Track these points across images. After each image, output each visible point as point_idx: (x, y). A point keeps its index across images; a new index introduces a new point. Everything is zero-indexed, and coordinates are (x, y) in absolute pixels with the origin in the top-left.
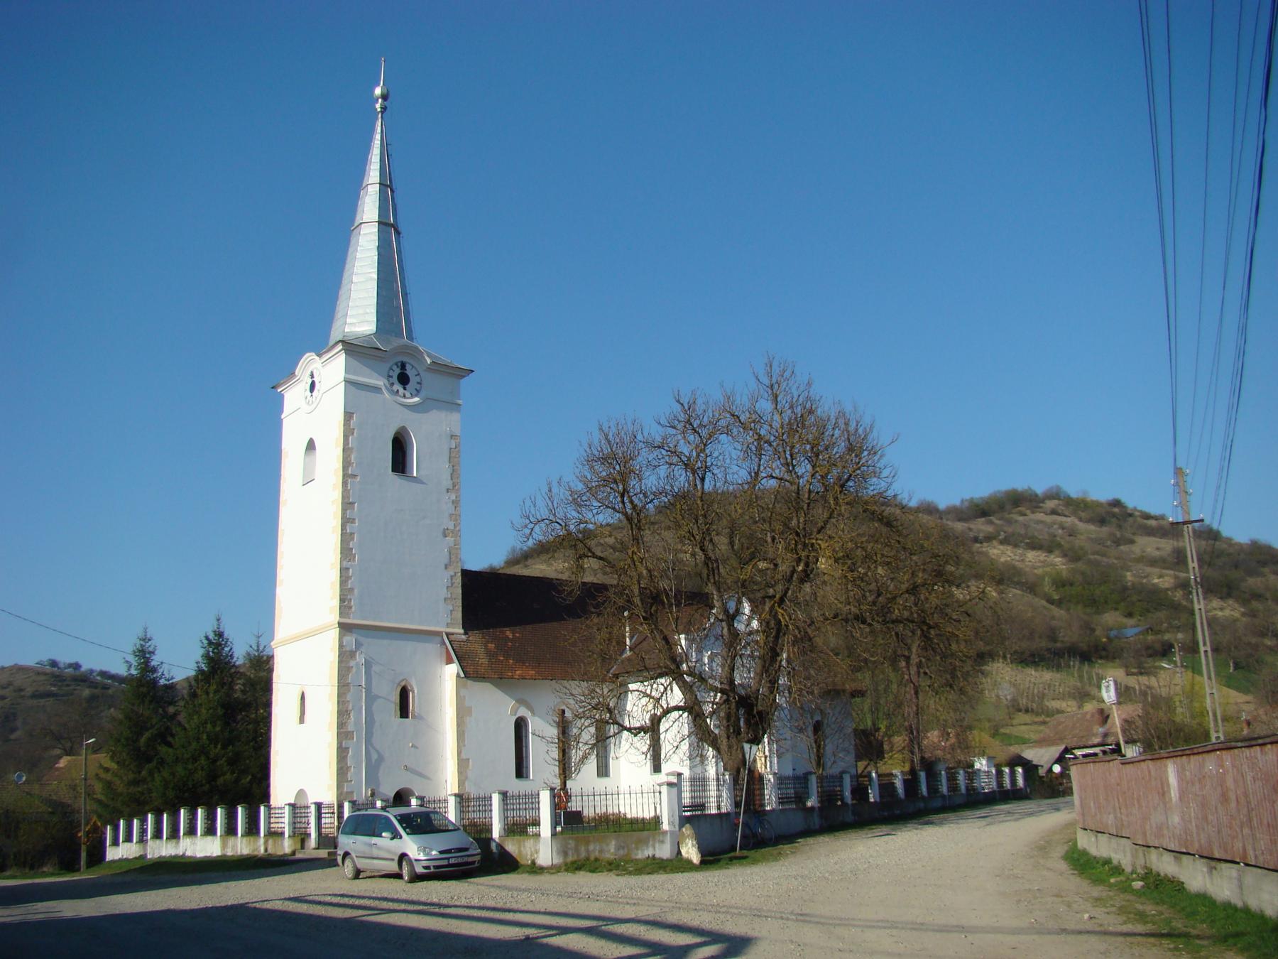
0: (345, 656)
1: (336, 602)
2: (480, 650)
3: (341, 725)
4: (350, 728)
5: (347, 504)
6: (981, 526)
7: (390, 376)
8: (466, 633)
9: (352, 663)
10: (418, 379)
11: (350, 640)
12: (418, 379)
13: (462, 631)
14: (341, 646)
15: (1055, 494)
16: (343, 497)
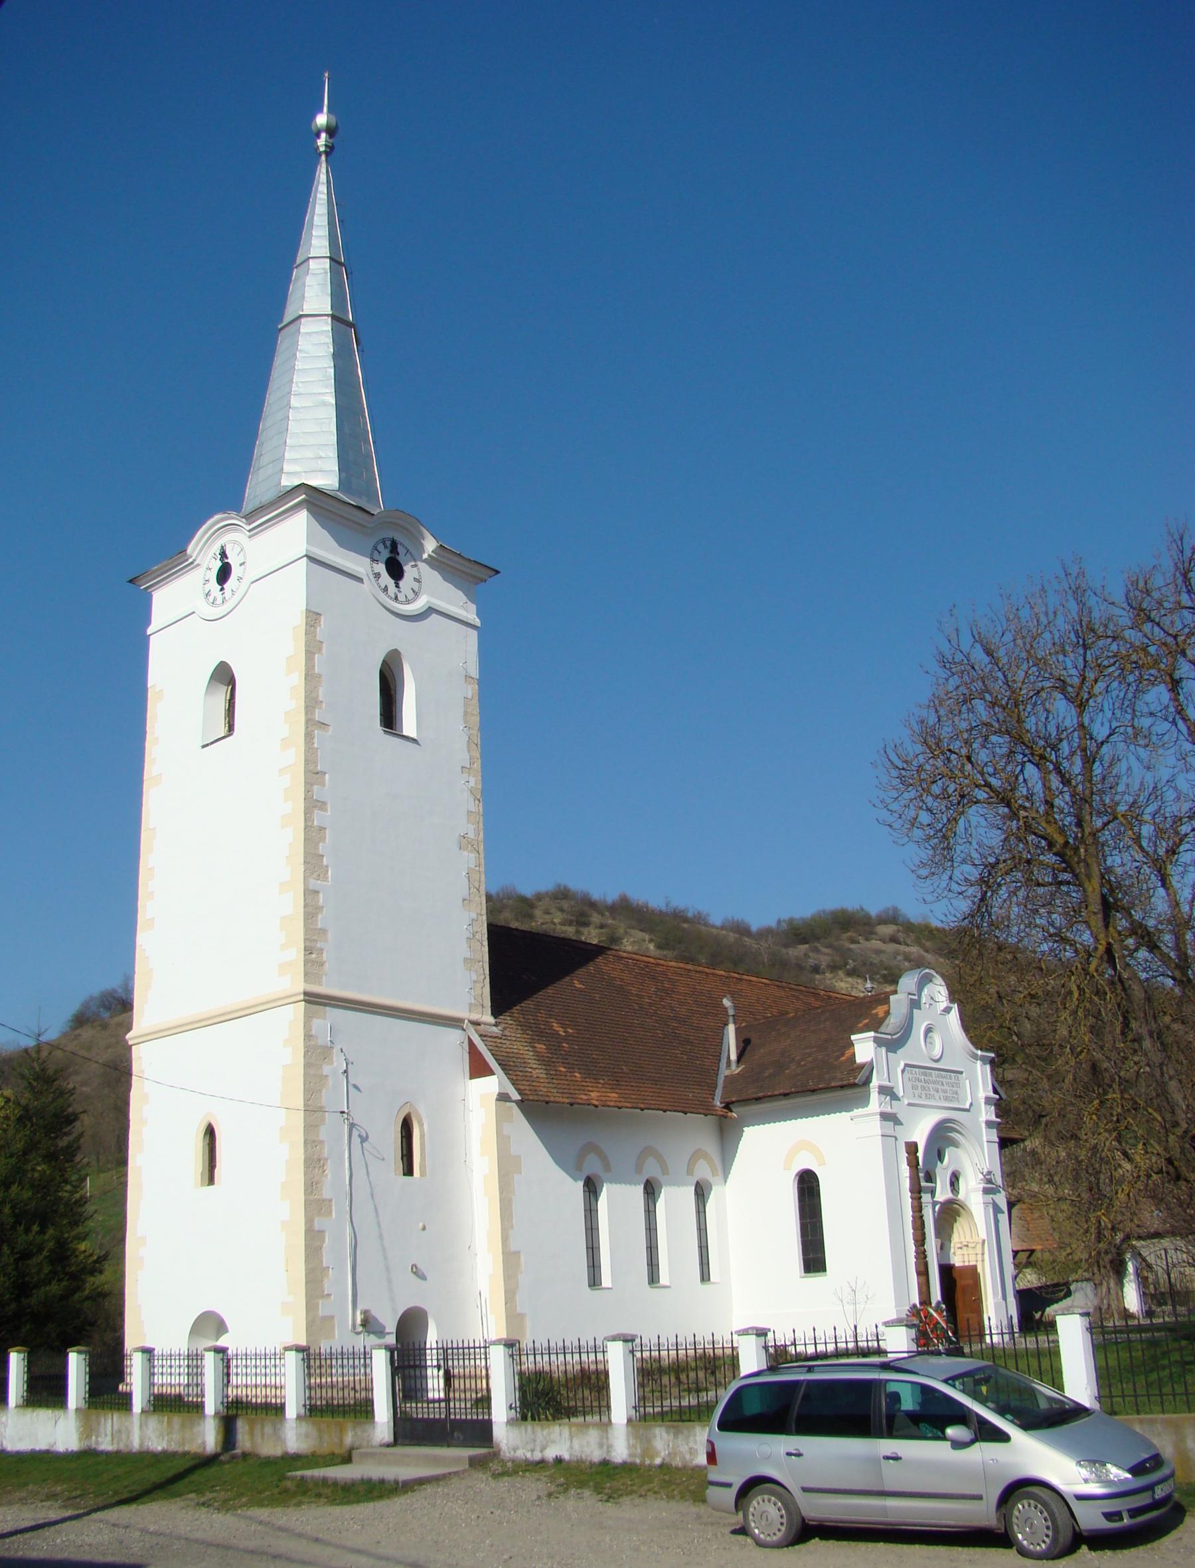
0: (316, 1054)
1: (296, 954)
3: (311, 1186)
4: (327, 1193)
5: (313, 776)
6: (798, 951)
9: (326, 1069)
14: (308, 1036)
15: (891, 918)
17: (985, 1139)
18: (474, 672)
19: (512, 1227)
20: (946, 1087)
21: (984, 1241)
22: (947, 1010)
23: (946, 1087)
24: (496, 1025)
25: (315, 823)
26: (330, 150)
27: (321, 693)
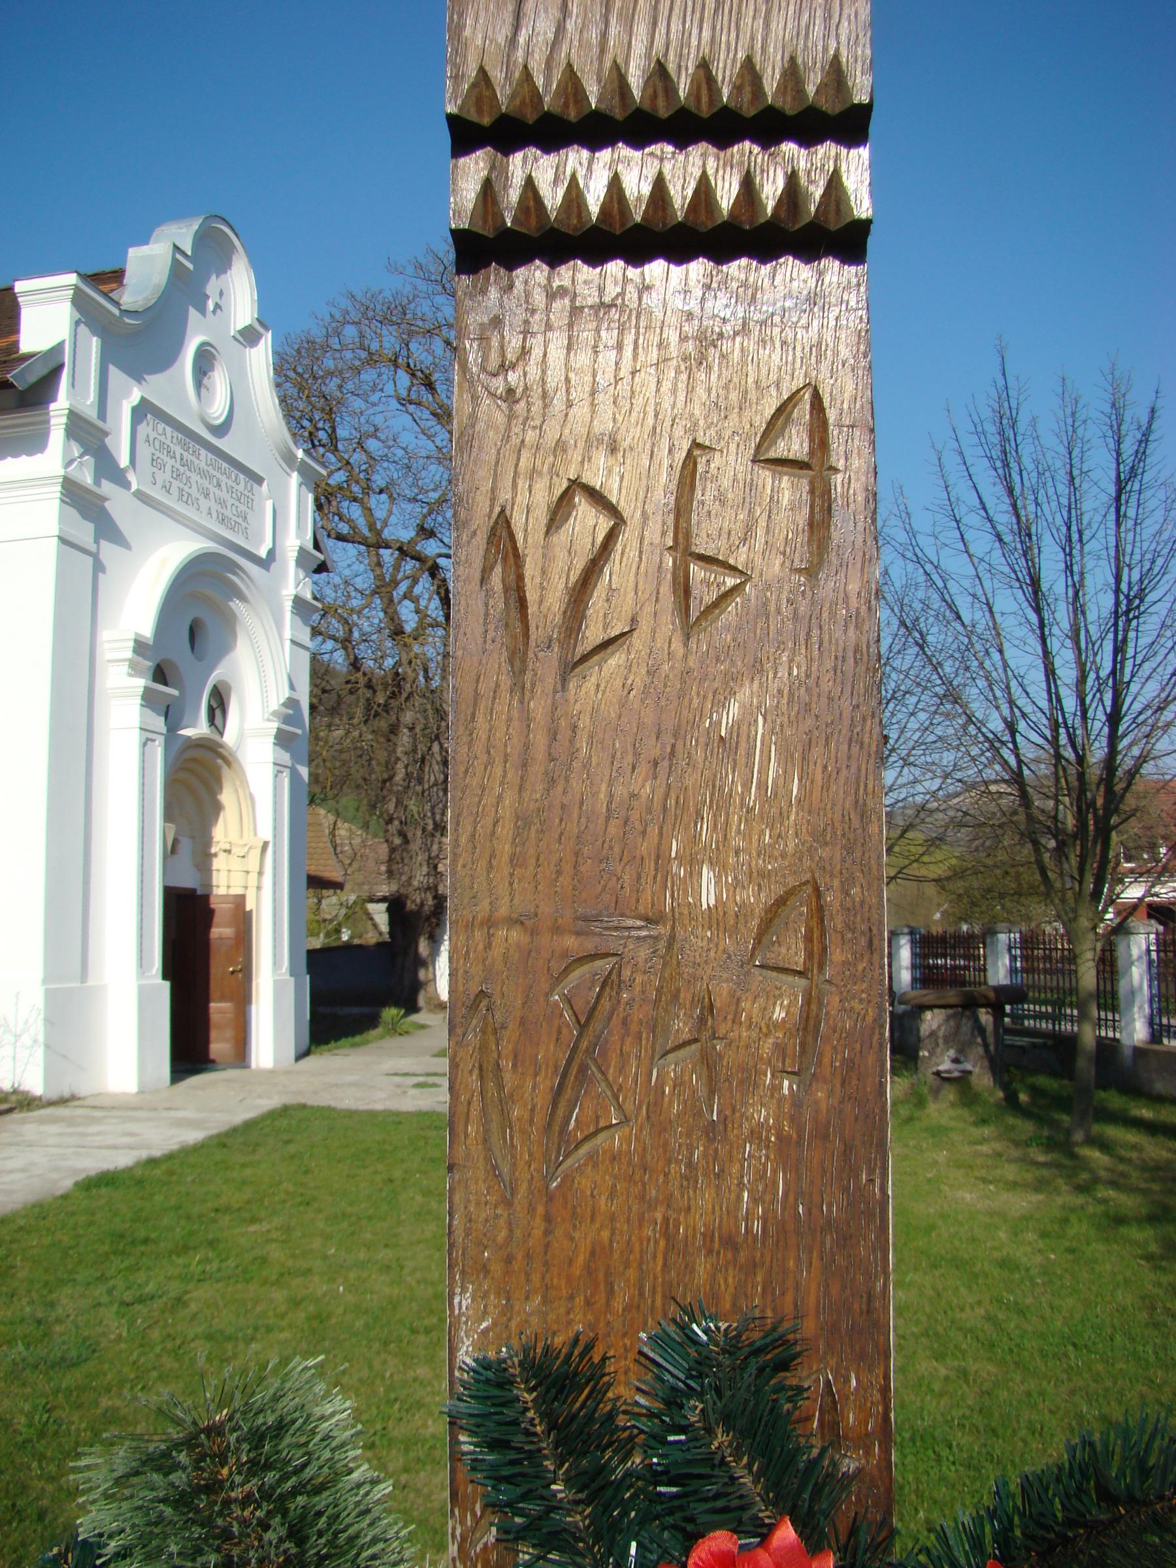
17: (288, 634)
20: (224, 495)
21: (266, 844)
22: (249, 336)
23: (224, 495)
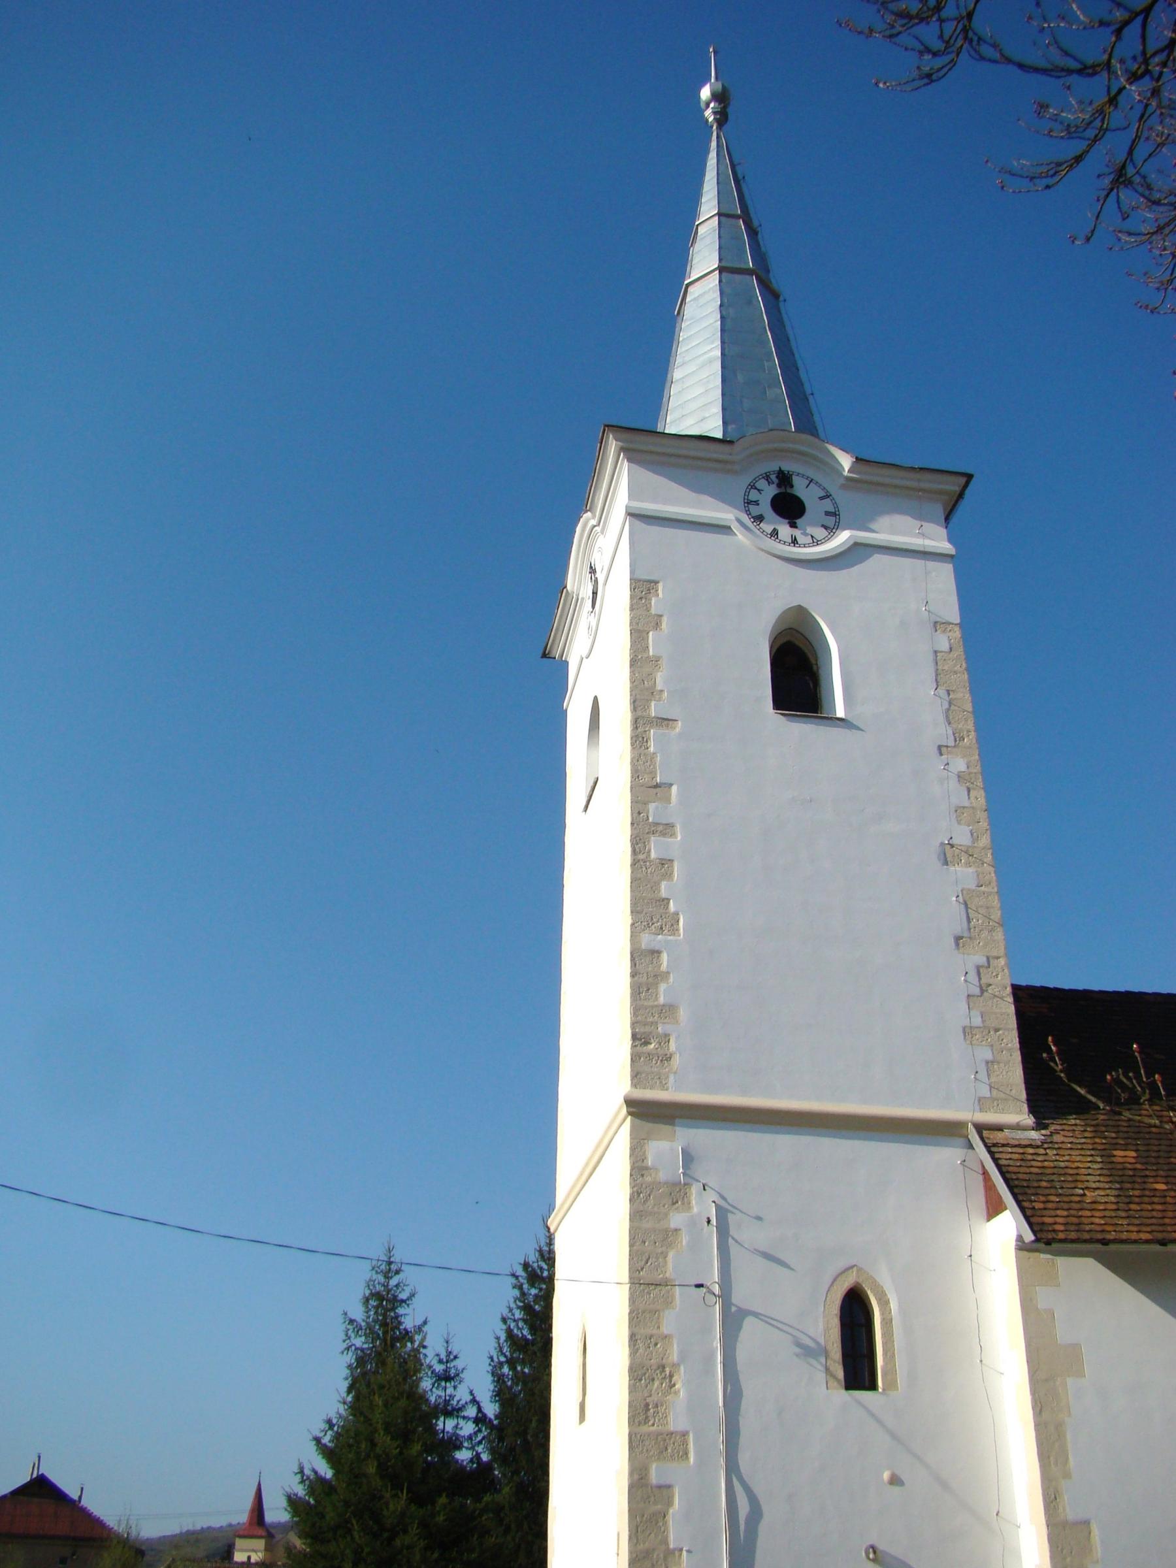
2: (1090, 1168)
4: (677, 1419)
7: (759, 519)
8: (1039, 1126)
9: (677, 1219)
10: (827, 505)
11: (666, 1148)
12: (827, 505)
13: (1030, 1120)
14: (639, 1169)
16: (636, 774)
18: (951, 612)
19: (1067, 1475)
24: (1039, 1126)
25: (653, 855)
26: (722, 118)
27: (660, 680)
